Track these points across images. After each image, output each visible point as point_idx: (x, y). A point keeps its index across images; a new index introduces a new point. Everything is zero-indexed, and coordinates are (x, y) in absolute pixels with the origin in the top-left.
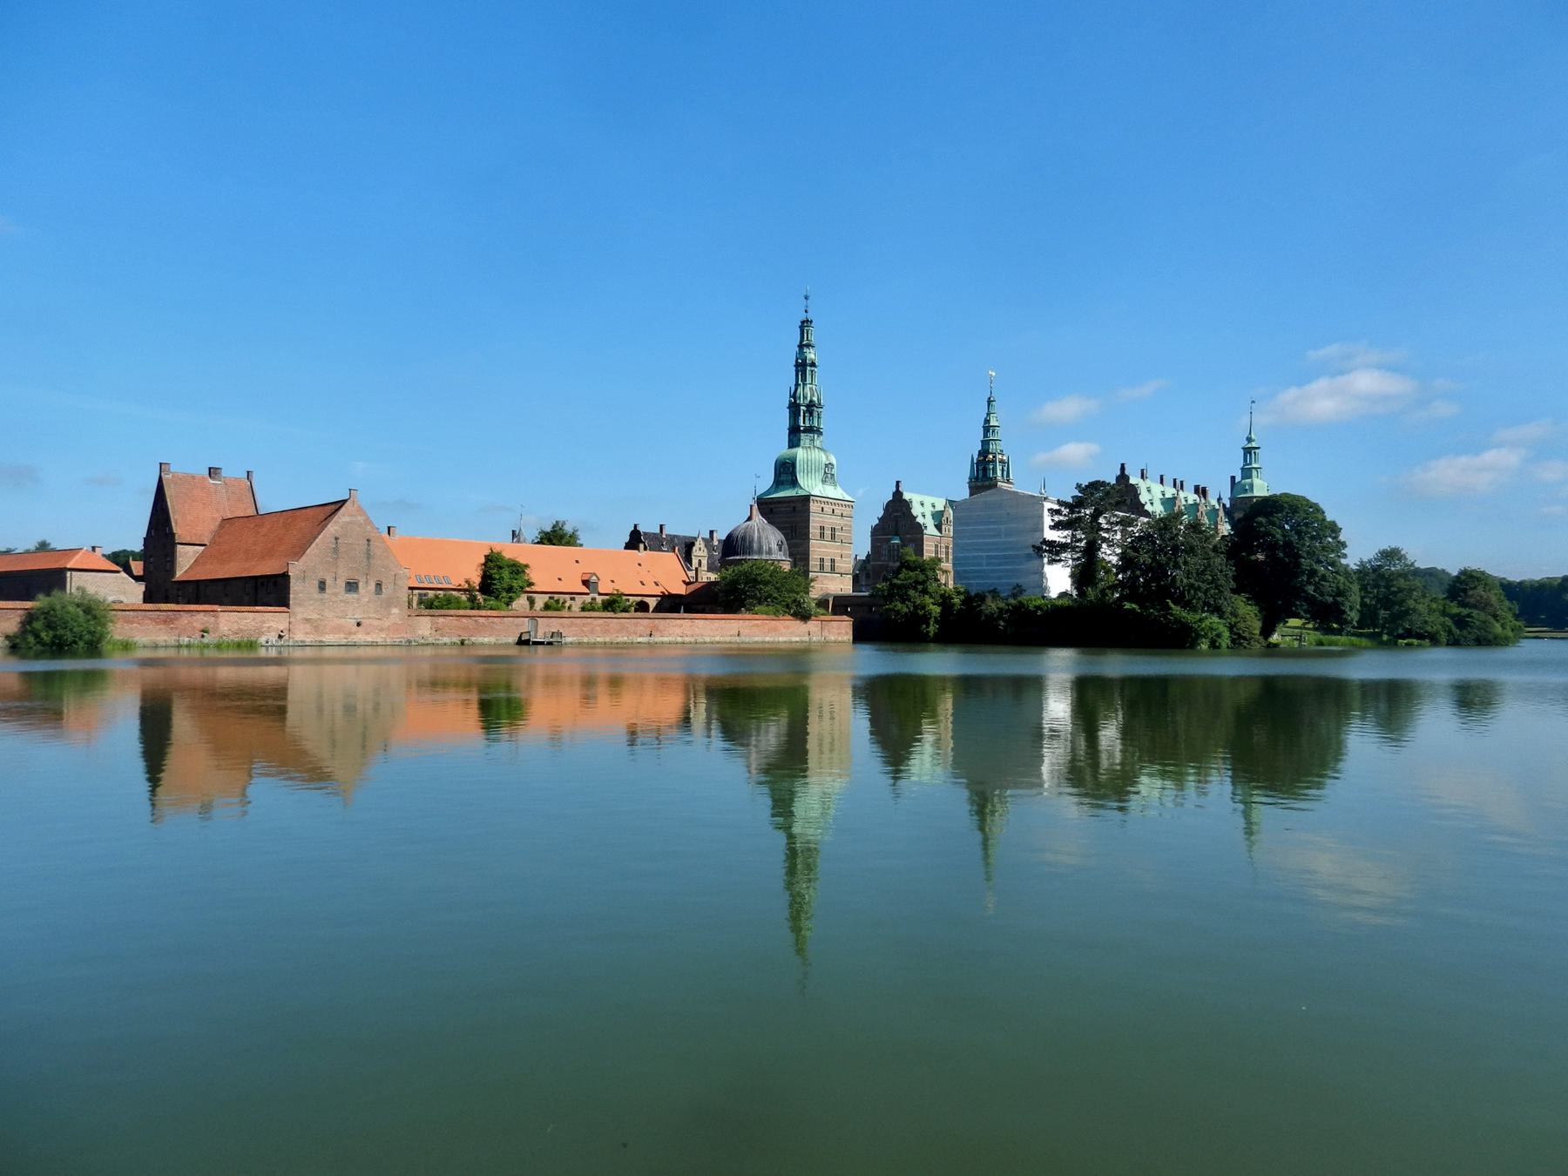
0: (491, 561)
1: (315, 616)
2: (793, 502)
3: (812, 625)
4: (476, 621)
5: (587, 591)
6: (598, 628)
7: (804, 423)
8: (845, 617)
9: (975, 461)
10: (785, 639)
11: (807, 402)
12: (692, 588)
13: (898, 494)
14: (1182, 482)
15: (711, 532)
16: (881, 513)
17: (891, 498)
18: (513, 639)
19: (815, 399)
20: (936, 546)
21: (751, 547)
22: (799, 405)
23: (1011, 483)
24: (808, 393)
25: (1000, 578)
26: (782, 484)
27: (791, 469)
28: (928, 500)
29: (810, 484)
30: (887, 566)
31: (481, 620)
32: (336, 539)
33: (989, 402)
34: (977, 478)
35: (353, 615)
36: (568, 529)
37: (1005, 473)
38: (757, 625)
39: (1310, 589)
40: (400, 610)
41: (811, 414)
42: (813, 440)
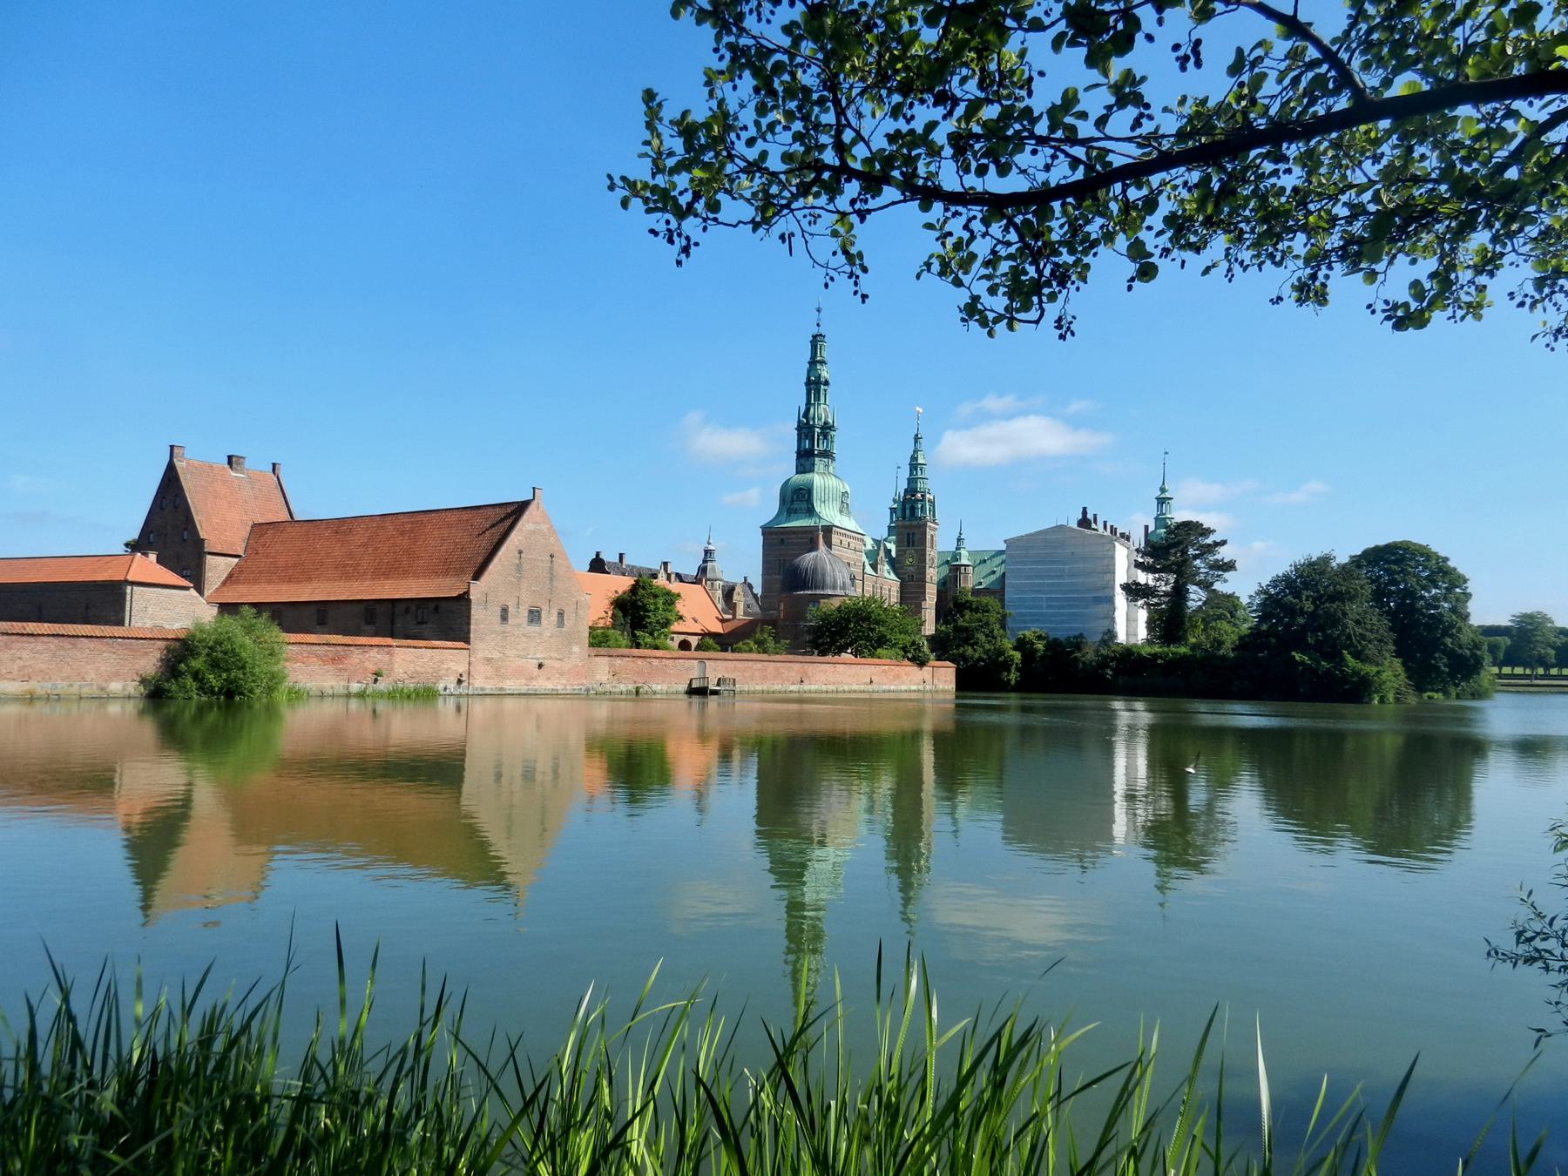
0: (644, 588)
1: (496, 655)
4: (650, 663)
6: (757, 673)
11: (822, 423)
15: (665, 564)
18: (683, 687)
19: (830, 421)
23: (936, 523)
24: (823, 412)
25: (1062, 622)
26: (795, 513)
31: (656, 662)
32: (520, 552)
33: (917, 439)
35: (535, 654)
38: (884, 671)
40: (581, 648)
42: (827, 466)
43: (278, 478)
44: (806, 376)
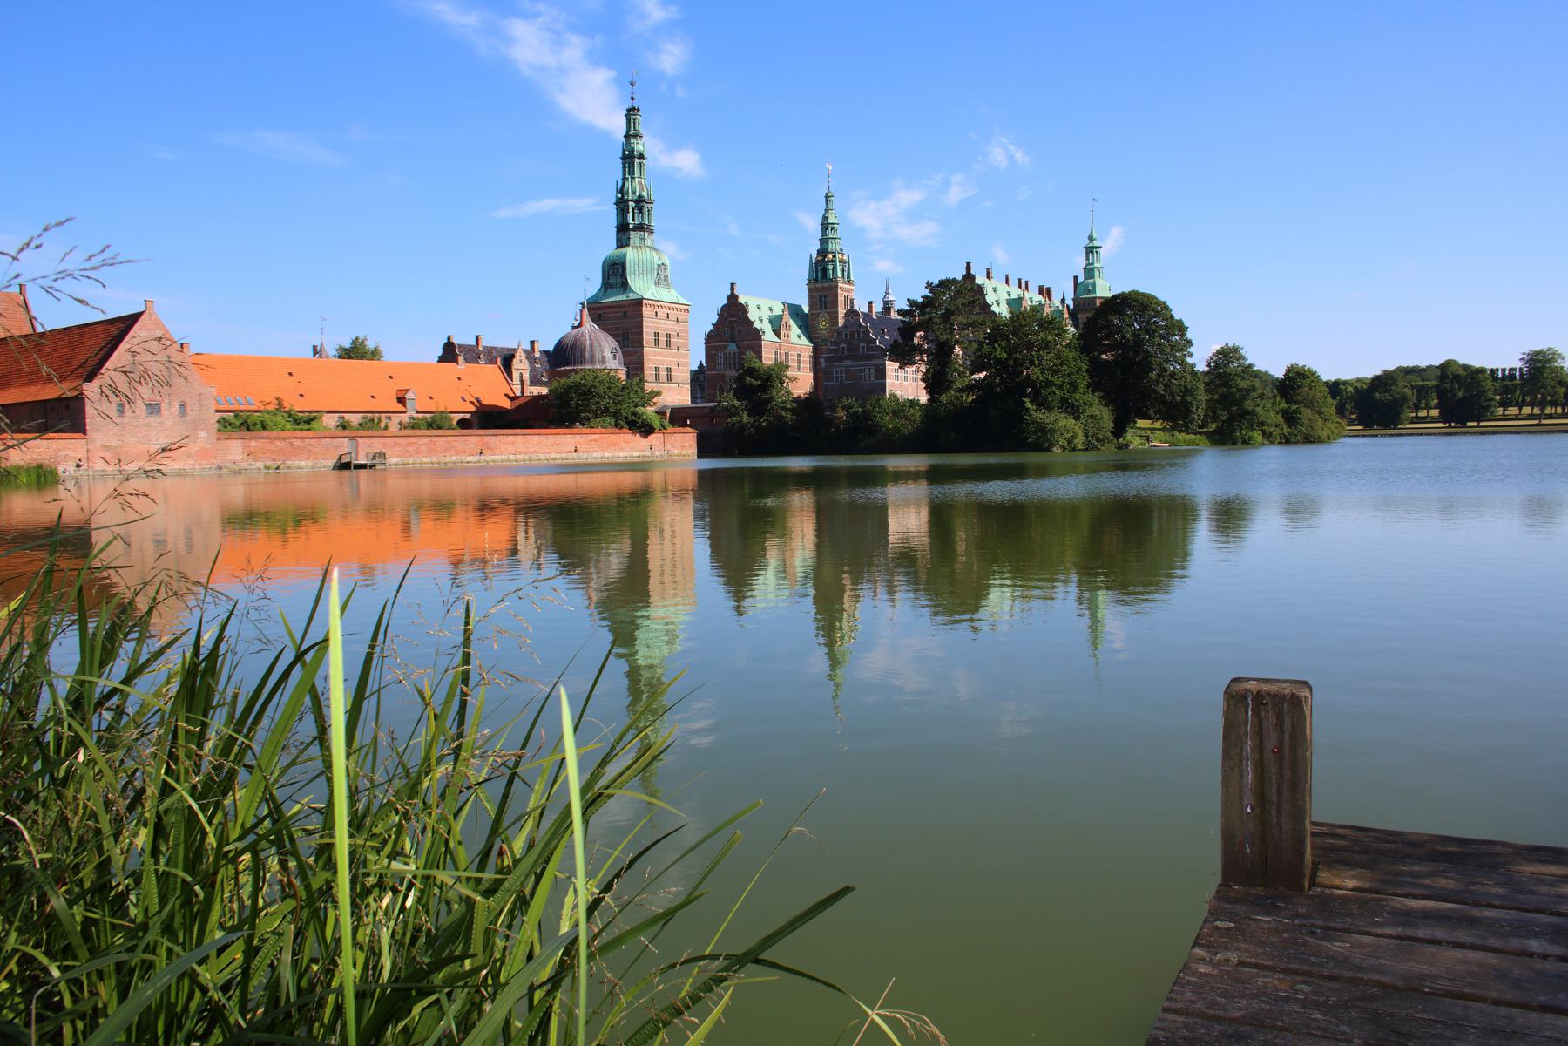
1: (115, 443)
2: (624, 306)
3: (655, 439)
5: (403, 409)
6: (423, 448)
7: (633, 220)
8: (689, 429)
9: (814, 261)
10: (625, 454)
11: (635, 198)
12: (518, 403)
13: (733, 297)
14: (1027, 282)
15: (532, 343)
16: (715, 318)
17: (725, 302)
18: (331, 463)
19: (645, 194)
20: (776, 353)
21: (582, 356)
22: (628, 201)
23: (852, 284)
24: (637, 187)
27: (621, 271)
28: (765, 304)
29: (642, 287)
30: (724, 376)
31: (297, 442)
33: (827, 197)
34: (816, 280)
35: (158, 440)
36: (370, 345)
37: (846, 273)
38: (596, 440)
39: (1160, 389)
40: (208, 433)
41: (641, 211)
42: (643, 239)
43: (24, 297)
44: (621, 150)
